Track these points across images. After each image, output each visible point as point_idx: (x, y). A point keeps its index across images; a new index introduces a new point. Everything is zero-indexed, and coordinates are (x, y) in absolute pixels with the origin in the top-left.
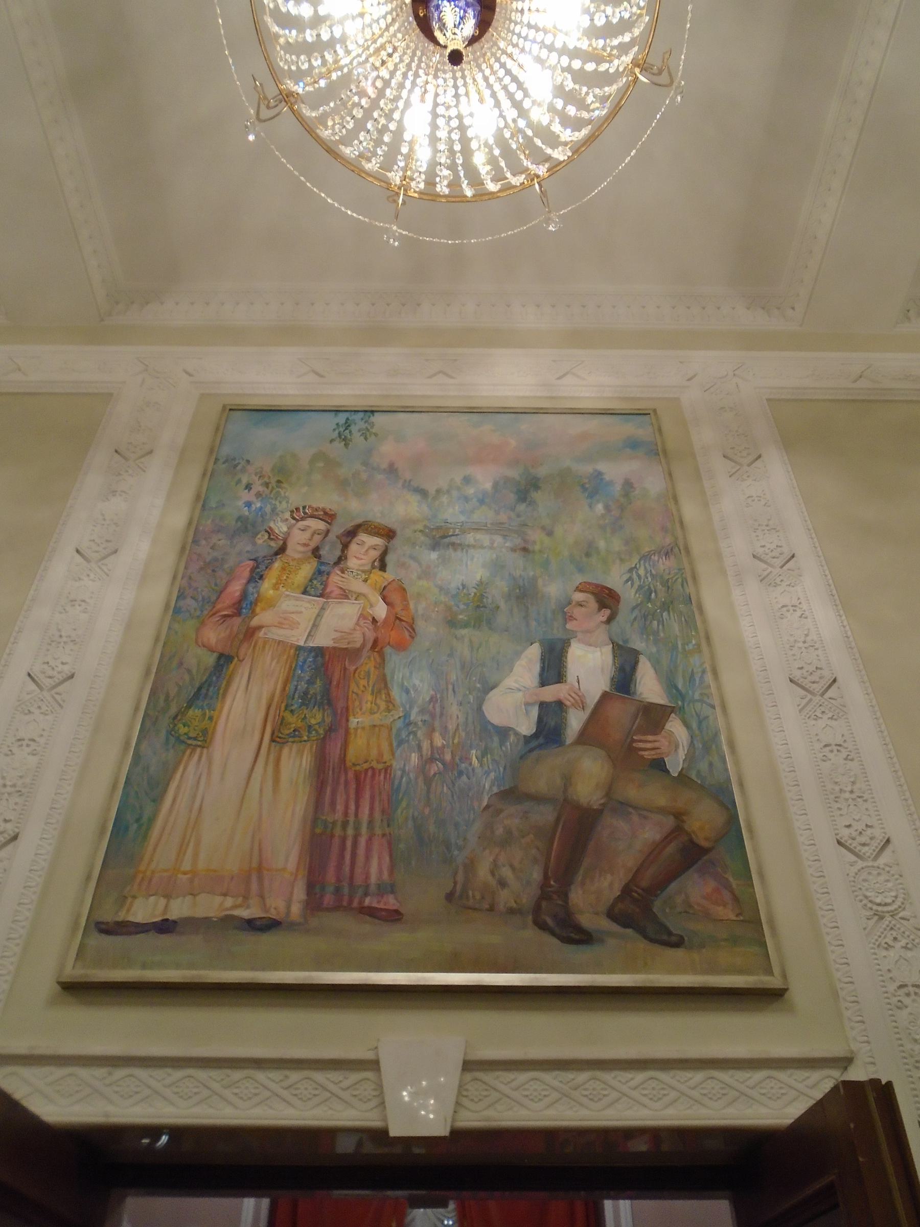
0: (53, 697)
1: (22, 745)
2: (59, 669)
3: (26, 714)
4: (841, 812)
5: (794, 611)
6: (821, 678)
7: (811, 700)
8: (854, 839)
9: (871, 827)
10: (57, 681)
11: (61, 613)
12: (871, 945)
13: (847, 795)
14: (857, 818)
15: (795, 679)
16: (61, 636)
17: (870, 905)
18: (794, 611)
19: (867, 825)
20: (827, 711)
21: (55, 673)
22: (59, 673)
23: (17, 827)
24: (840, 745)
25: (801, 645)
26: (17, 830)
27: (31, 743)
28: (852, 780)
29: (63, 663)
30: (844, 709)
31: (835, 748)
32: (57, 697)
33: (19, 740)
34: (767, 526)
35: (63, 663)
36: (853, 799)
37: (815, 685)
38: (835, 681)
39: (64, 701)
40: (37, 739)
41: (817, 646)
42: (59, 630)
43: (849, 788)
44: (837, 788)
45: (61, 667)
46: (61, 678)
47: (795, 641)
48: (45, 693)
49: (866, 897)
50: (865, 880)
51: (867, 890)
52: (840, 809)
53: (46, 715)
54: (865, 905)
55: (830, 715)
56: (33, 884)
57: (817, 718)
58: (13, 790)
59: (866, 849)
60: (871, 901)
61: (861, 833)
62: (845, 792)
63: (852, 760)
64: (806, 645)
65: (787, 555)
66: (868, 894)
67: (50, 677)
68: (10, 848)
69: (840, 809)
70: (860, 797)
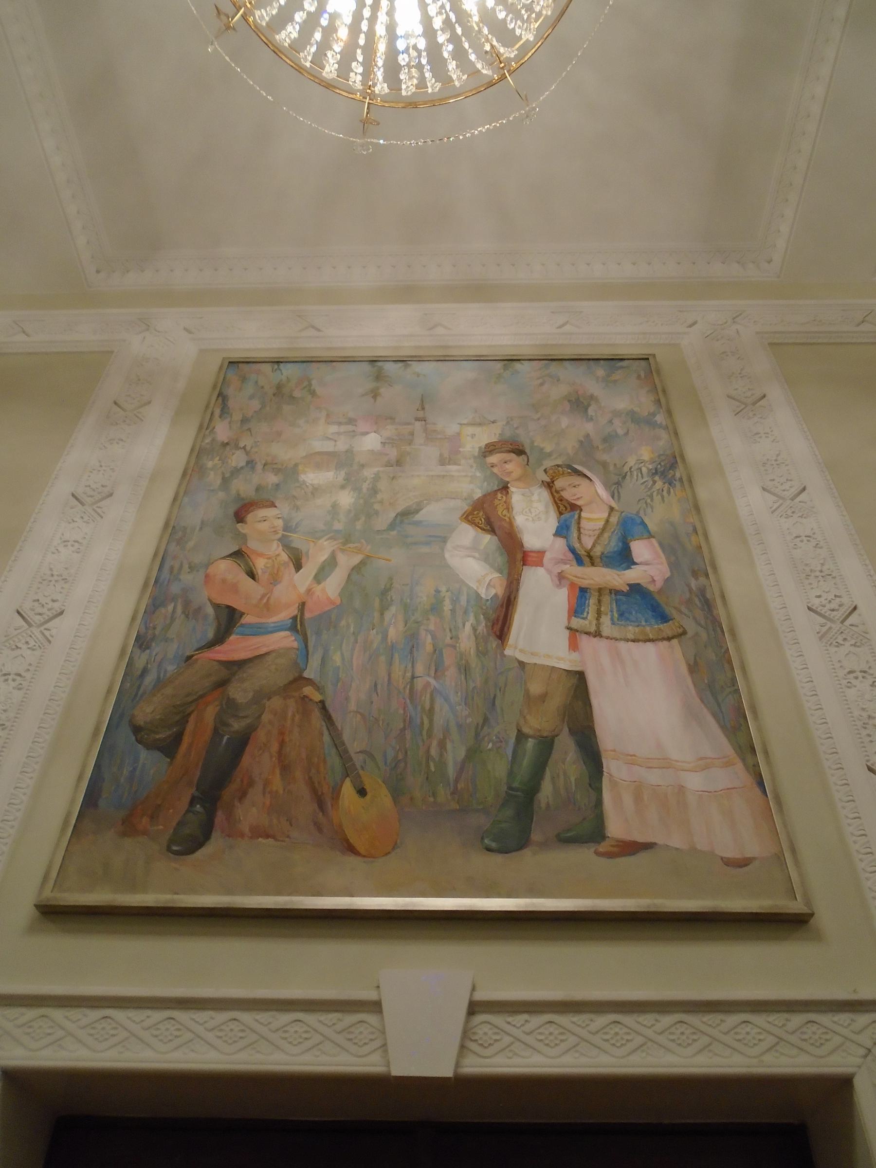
0: (43, 634)
1: (6, 680)
2: (49, 606)
3: (13, 650)
4: (870, 739)
6: (840, 606)
7: (830, 628)
10: (47, 618)
11: (53, 553)
15: (814, 608)
16: (52, 575)
18: (808, 541)
20: (849, 638)
21: (44, 610)
22: (49, 610)
24: (865, 672)
25: (818, 574)
27: (18, 678)
29: (53, 601)
30: (867, 636)
31: (860, 675)
33: (5, 675)
35: (53, 601)
37: (835, 613)
38: (855, 608)
39: (52, 636)
40: (23, 674)
41: (834, 575)
42: (51, 569)
44: (865, 714)
45: (51, 605)
46: (51, 615)
47: (811, 571)
48: (34, 629)
53: (33, 650)
55: (853, 642)
56: (11, 818)
57: (839, 645)
67: (40, 614)
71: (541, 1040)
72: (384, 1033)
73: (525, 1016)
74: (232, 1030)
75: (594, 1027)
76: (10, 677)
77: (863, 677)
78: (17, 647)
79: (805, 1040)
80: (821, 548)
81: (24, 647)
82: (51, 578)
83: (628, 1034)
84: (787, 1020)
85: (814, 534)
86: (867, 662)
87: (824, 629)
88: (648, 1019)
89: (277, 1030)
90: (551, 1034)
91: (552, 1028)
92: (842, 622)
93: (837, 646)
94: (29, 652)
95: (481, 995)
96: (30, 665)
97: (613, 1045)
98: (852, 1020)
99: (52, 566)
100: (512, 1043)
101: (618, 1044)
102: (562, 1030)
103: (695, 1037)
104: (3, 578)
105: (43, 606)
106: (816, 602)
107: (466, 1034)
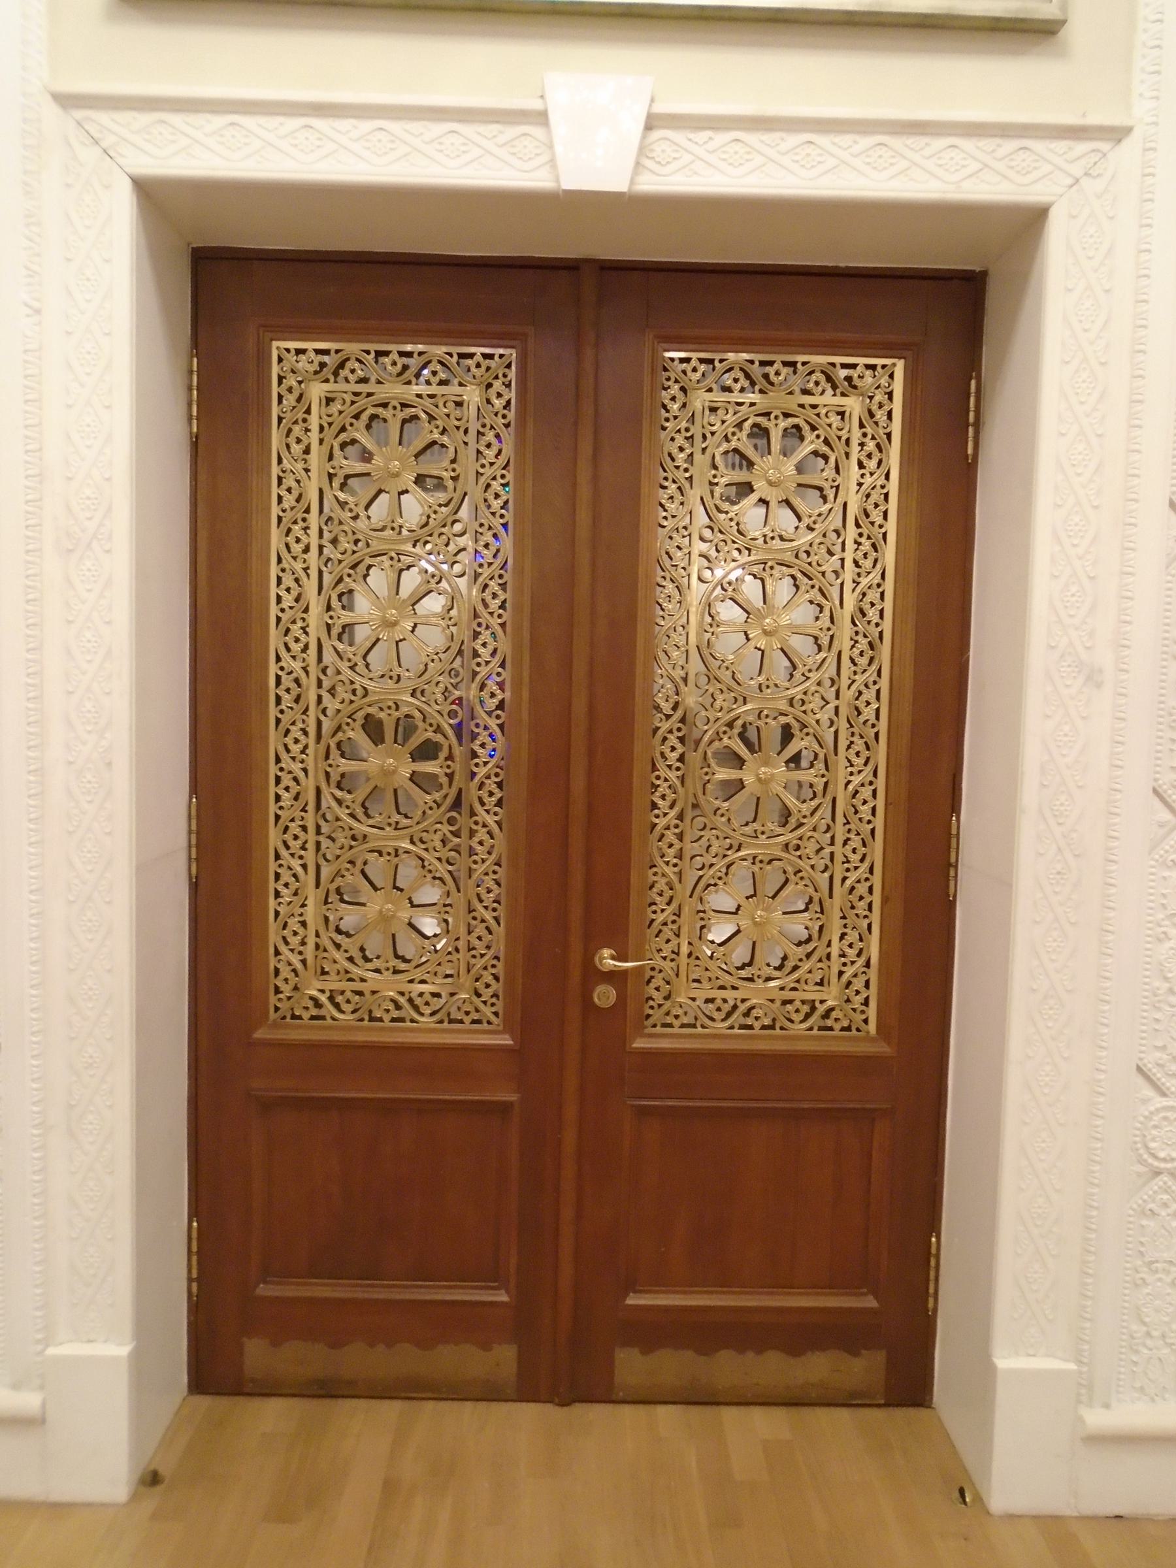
71: (724, 160)
72: (551, 147)
73: (709, 133)
74: (380, 141)
75: (784, 147)
79: (1012, 168)
83: (821, 155)
84: (999, 146)
88: (845, 140)
89: (433, 141)
90: (736, 153)
91: (737, 147)
95: (660, 108)
97: (803, 166)
98: (1070, 148)
100: (693, 162)
101: (808, 166)
102: (749, 149)
103: (893, 161)
107: (642, 150)
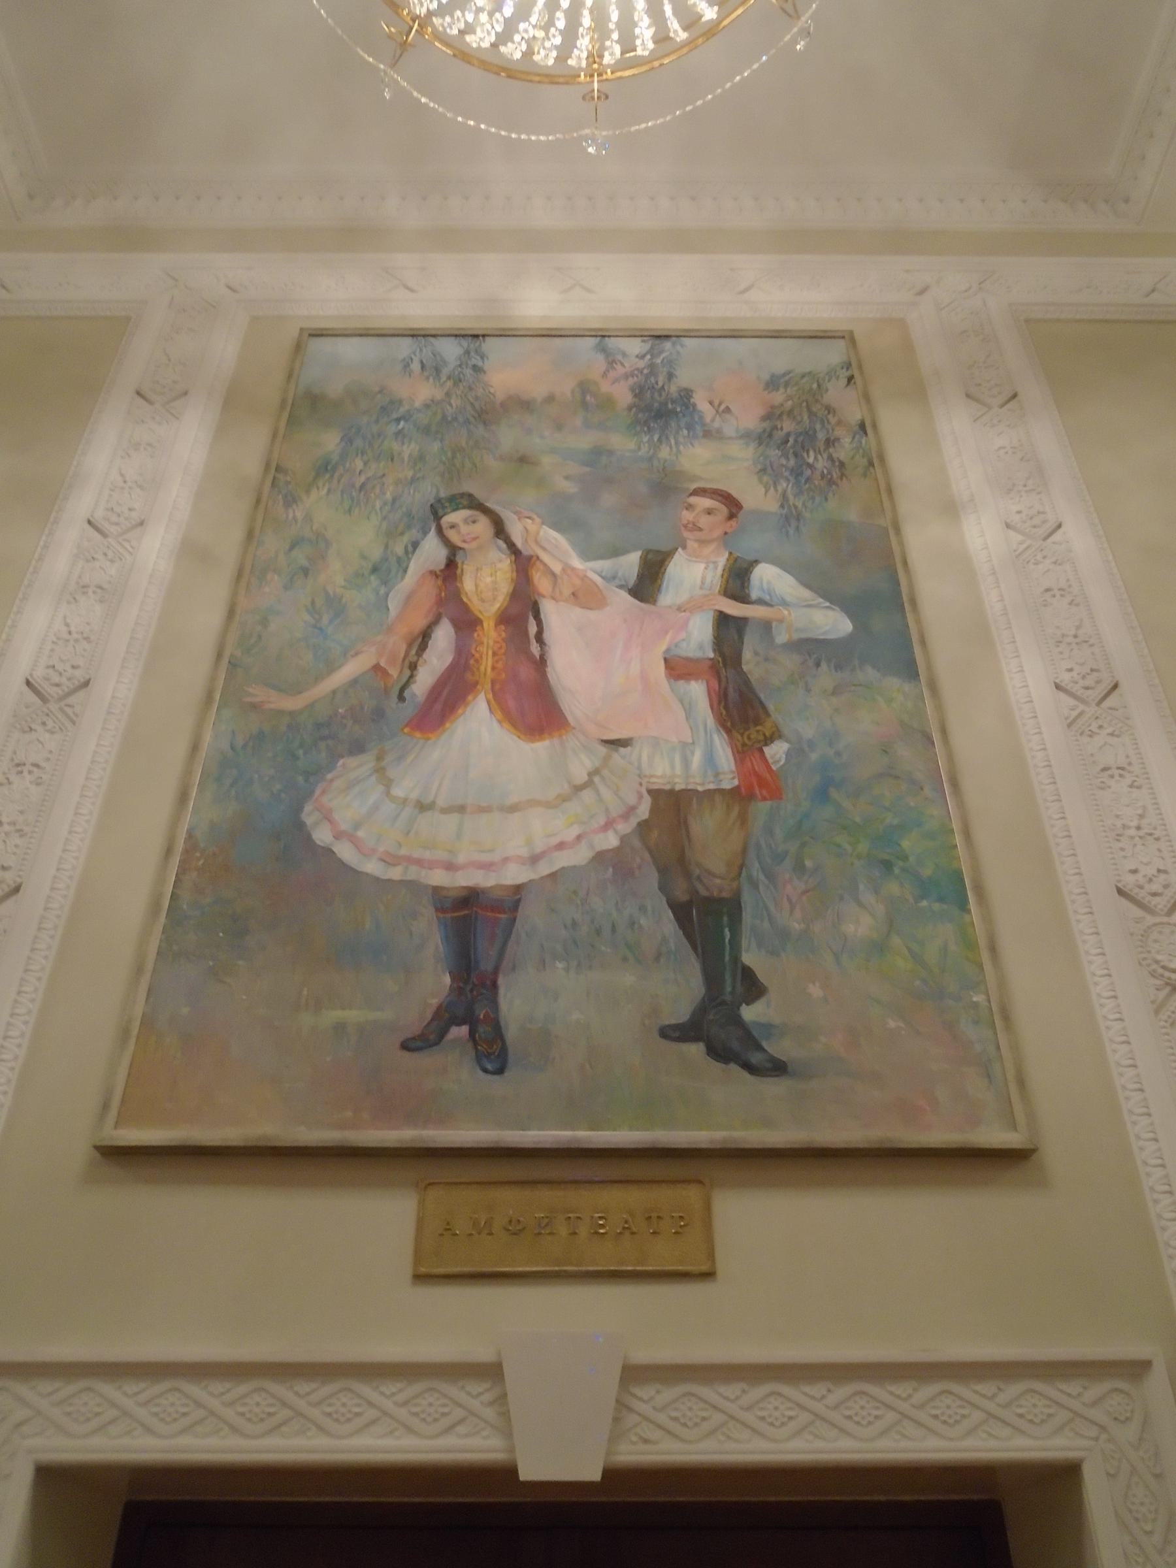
1: (21, 772)
3: (24, 732)
4: (1123, 854)
5: (1062, 596)
6: (1098, 682)
8: (1141, 887)
9: (1165, 872)
12: (1162, 1023)
13: (1132, 832)
14: (1145, 860)
16: (70, 633)
17: (1161, 971)
18: (1062, 596)
19: (1159, 871)
20: (1105, 725)
21: (64, 680)
22: (69, 679)
23: (19, 876)
24: (1123, 769)
26: (19, 880)
27: (35, 770)
28: (1140, 812)
29: (73, 667)
31: (1117, 772)
32: (67, 710)
33: (18, 765)
34: (1025, 486)
36: (1141, 837)
37: (1090, 692)
39: (77, 715)
40: (43, 764)
42: (67, 625)
43: (1135, 823)
47: (1063, 635)
49: (1157, 962)
50: (1156, 941)
51: (1158, 952)
52: (1122, 849)
54: (1154, 971)
55: (1110, 730)
57: (1092, 735)
58: (12, 828)
59: (1157, 899)
60: (1163, 967)
61: (1150, 880)
62: (1129, 828)
63: (1139, 787)
64: (1077, 640)
65: (1051, 525)
66: (1159, 957)
67: (57, 685)
68: (10, 902)
69: (1122, 849)
70: (1151, 834)
76: (25, 769)
77: (1121, 776)
78: (31, 729)
80: (1077, 605)
81: (40, 728)
82: (67, 636)
85: (1070, 586)
86: (1127, 757)
87: (1075, 713)
92: (1099, 703)
93: (1091, 736)
94: (47, 735)
96: (51, 752)
99: (68, 621)
104: (4, 636)
105: (61, 674)
106: (1065, 678)
